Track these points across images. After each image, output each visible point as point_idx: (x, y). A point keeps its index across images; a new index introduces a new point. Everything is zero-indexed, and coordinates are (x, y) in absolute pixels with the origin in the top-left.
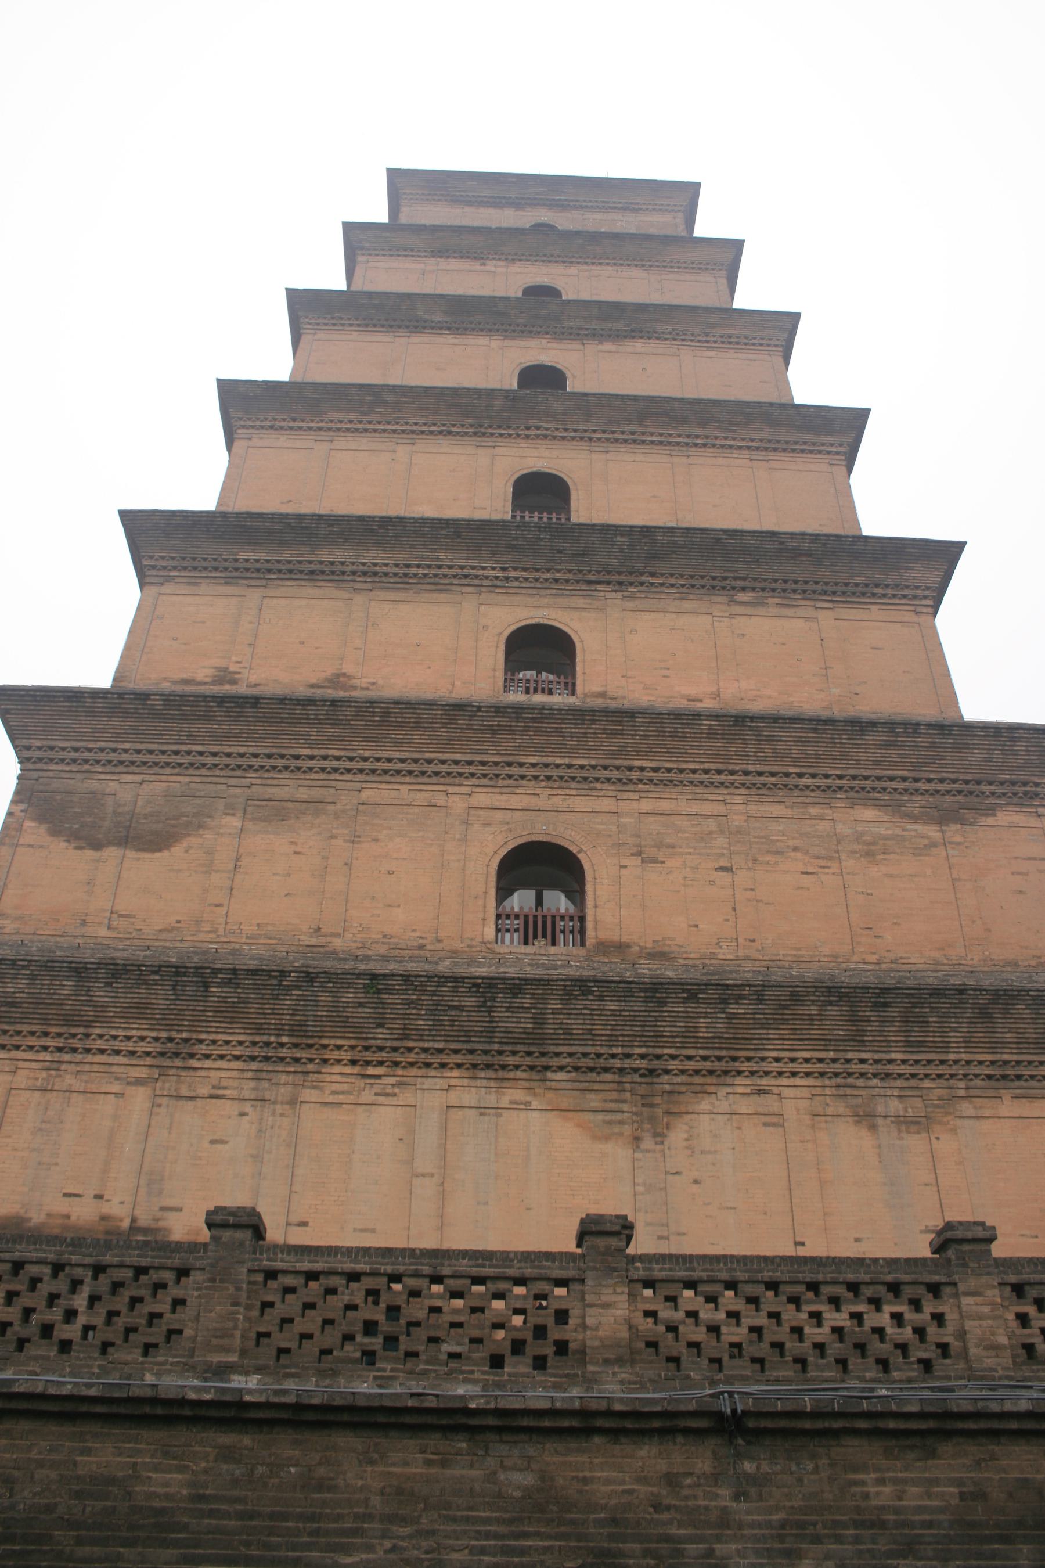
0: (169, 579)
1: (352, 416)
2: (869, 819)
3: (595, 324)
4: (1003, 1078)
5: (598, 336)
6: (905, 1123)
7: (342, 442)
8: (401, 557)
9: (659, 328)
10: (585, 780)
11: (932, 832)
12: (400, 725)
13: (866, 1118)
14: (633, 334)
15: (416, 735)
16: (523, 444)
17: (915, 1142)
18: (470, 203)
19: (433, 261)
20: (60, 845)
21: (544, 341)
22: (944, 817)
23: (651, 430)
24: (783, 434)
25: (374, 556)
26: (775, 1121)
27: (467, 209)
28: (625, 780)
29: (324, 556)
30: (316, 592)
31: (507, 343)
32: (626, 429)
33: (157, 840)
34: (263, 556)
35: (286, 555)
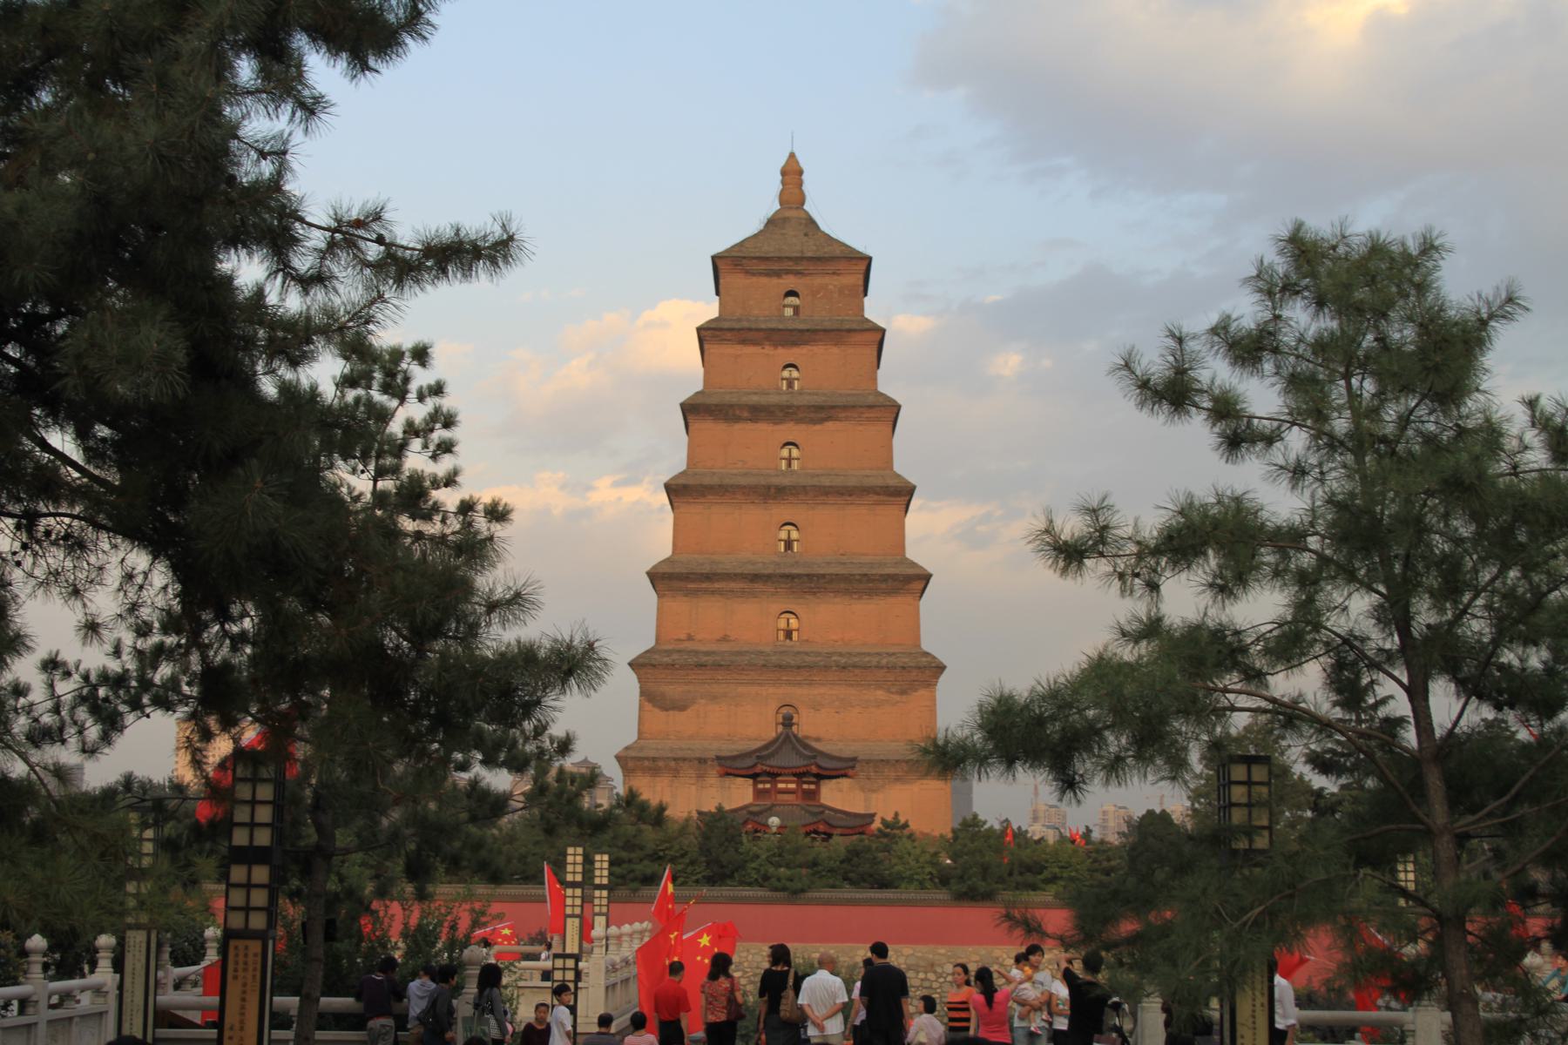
2: (880, 694)
4: (898, 779)
5: (814, 422)
6: (874, 791)
10: (799, 684)
11: (897, 698)
13: (862, 789)
14: (828, 419)
17: (874, 796)
19: (738, 347)
20: (657, 711)
22: (903, 692)
24: (882, 498)
25: (733, 585)
26: (841, 791)
27: (754, 279)
28: (811, 683)
29: (717, 585)
33: (683, 708)
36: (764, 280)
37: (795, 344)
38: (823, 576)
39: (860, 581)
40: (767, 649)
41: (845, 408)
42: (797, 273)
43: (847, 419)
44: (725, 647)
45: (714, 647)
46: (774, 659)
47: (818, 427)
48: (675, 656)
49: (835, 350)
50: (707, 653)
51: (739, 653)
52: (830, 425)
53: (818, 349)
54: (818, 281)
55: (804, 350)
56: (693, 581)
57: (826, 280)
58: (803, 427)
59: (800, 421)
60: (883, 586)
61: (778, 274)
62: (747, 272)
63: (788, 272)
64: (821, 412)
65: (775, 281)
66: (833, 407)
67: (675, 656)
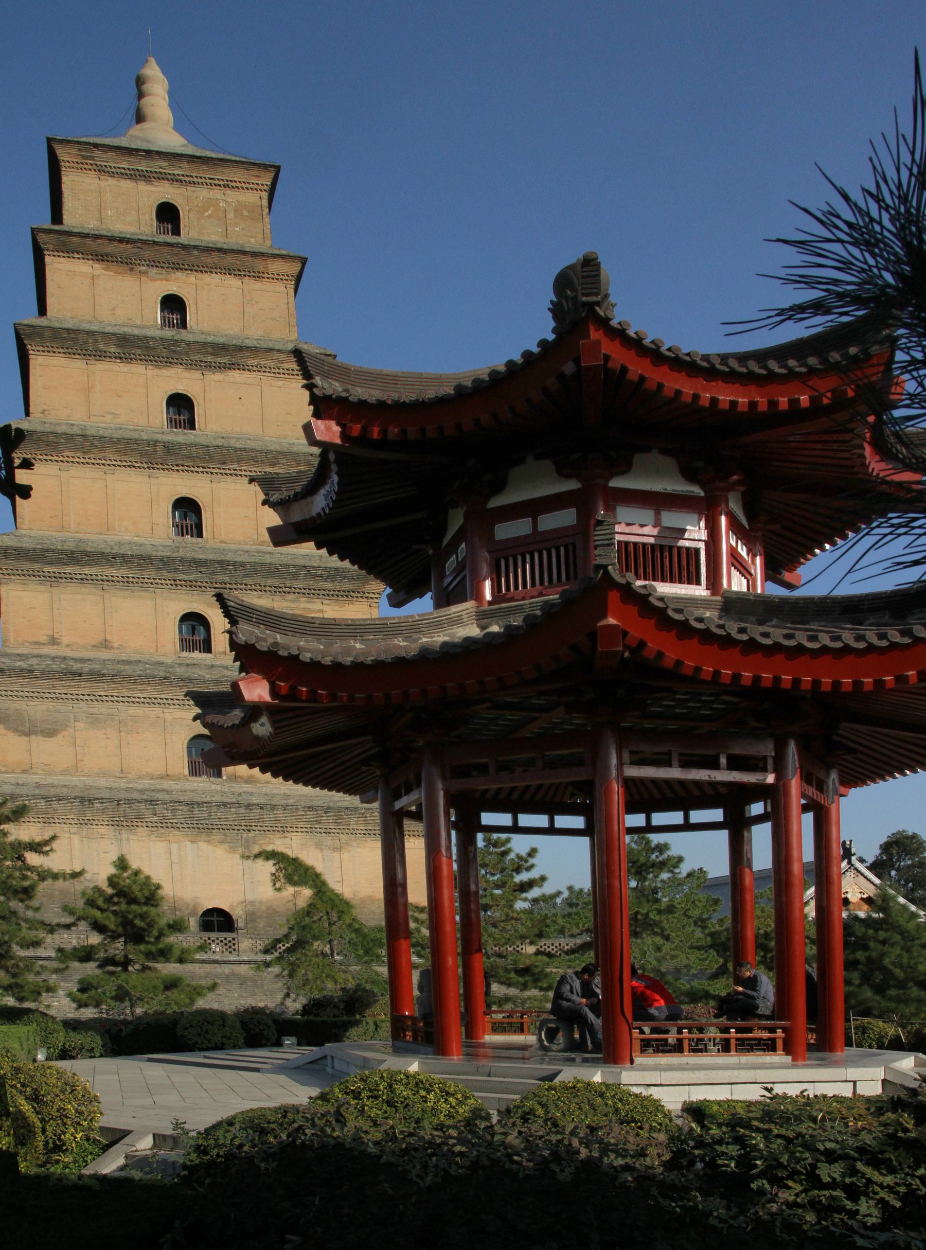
0: (11, 581)
1: (79, 454)
3: (209, 358)
7: (76, 471)
8: (124, 573)
9: (250, 362)
12: (142, 684)
14: (232, 366)
15: (149, 688)
16: (175, 474)
18: (112, 175)
19: (97, 266)
21: (180, 370)
23: (244, 468)
25: (111, 572)
27: (112, 181)
29: (87, 570)
30: (83, 590)
31: (156, 371)
32: (232, 467)
34: (56, 570)
35: (68, 569)
36: (126, 184)
37: (177, 267)
38: (243, 565)
39: (295, 576)
40: (169, 661)
41: (255, 350)
42: (175, 180)
43: (260, 369)
44: (104, 655)
45: (91, 655)
46: (180, 671)
47: (218, 376)
48: (34, 661)
49: (235, 282)
50: (82, 660)
51: (129, 662)
52: (236, 375)
53: (212, 280)
54: (203, 194)
55: (192, 278)
56: (51, 563)
57: (217, 194)
58: (198, 374)
59: (192, 365)
60: (328, 585)
61: (146, 177)
62: (102, 171)
63: (162, 177)
64: (226, 355)
65: (143, 187)
66: (240, 348)
67: (34, 661)
